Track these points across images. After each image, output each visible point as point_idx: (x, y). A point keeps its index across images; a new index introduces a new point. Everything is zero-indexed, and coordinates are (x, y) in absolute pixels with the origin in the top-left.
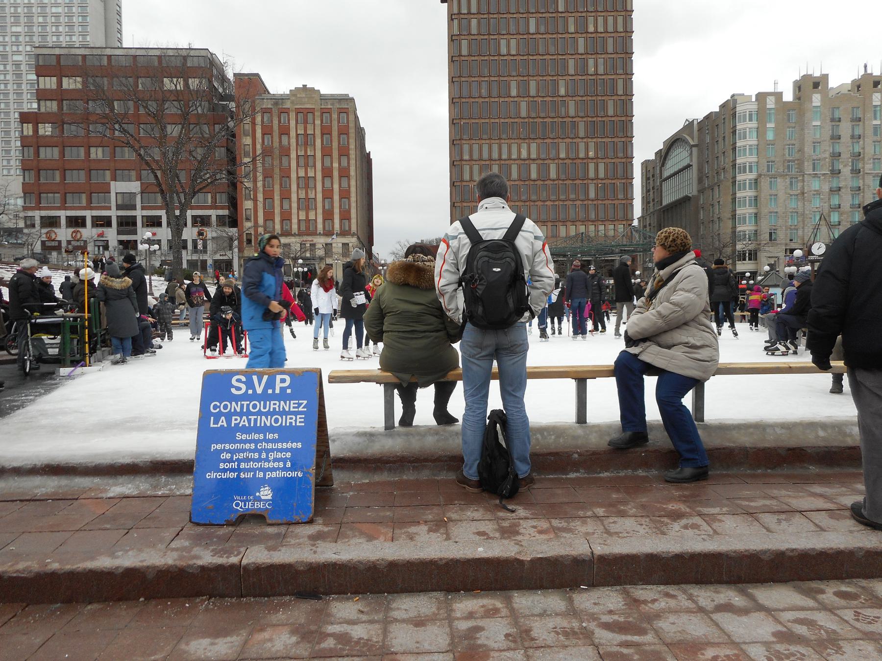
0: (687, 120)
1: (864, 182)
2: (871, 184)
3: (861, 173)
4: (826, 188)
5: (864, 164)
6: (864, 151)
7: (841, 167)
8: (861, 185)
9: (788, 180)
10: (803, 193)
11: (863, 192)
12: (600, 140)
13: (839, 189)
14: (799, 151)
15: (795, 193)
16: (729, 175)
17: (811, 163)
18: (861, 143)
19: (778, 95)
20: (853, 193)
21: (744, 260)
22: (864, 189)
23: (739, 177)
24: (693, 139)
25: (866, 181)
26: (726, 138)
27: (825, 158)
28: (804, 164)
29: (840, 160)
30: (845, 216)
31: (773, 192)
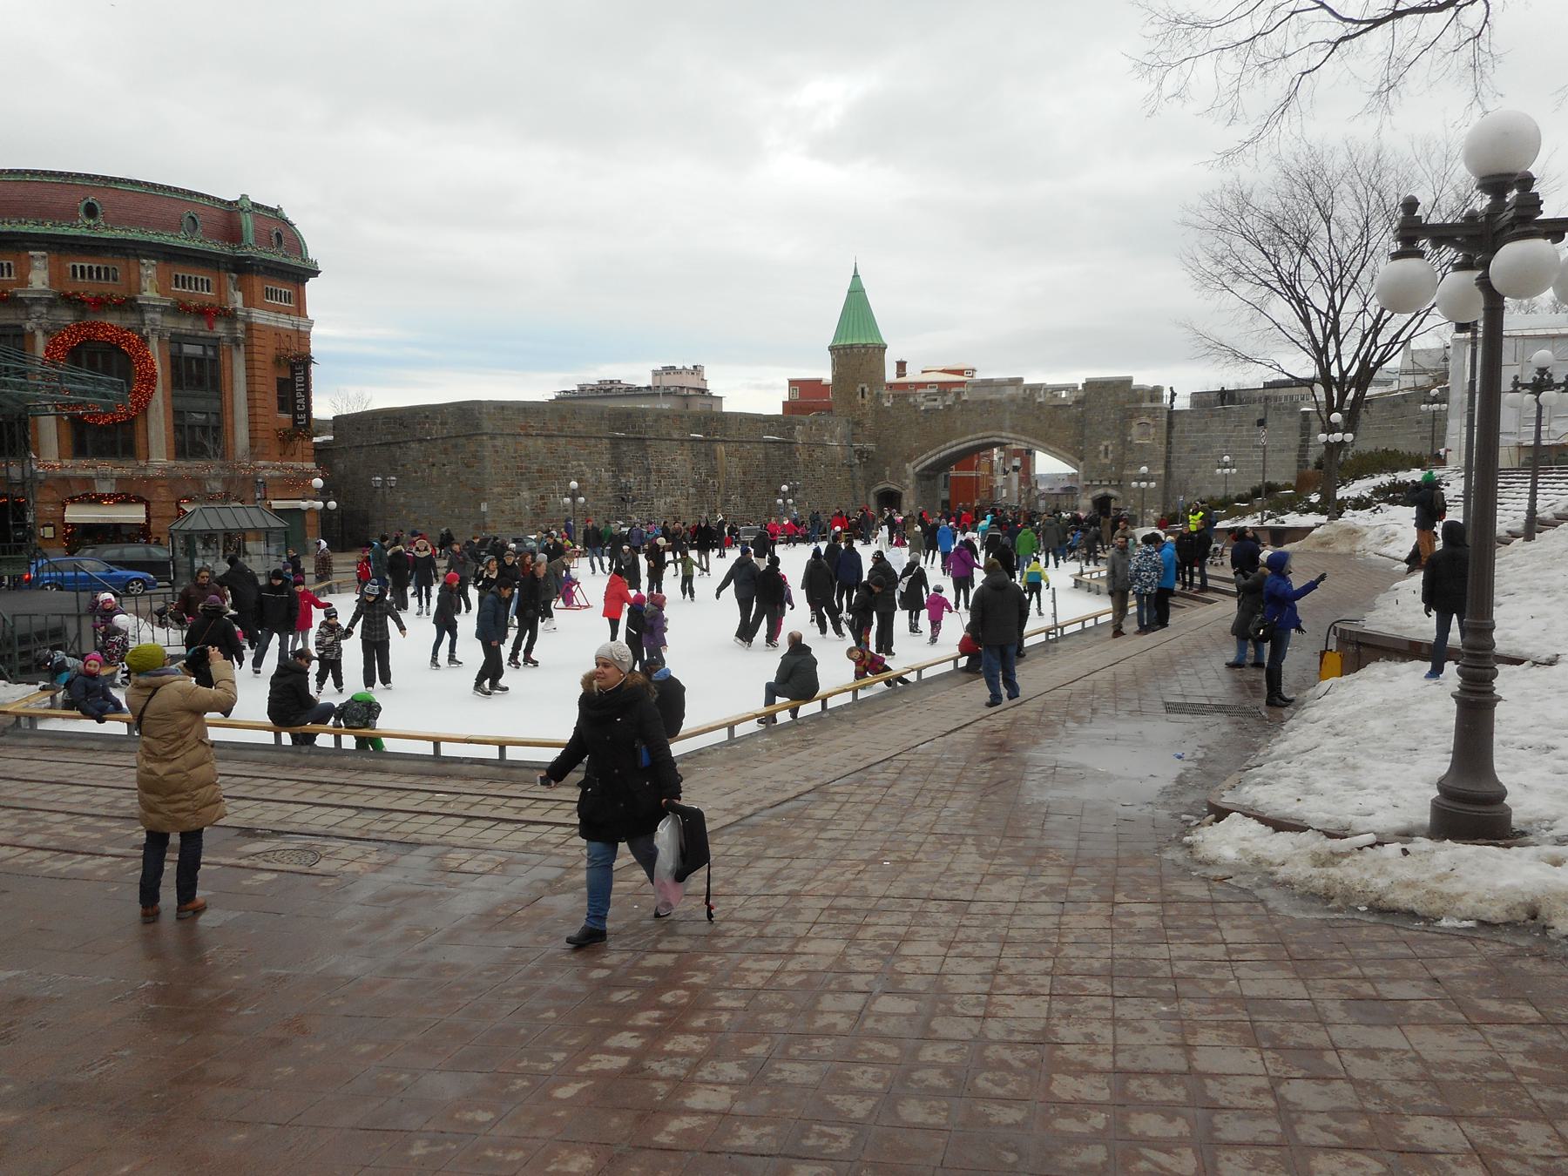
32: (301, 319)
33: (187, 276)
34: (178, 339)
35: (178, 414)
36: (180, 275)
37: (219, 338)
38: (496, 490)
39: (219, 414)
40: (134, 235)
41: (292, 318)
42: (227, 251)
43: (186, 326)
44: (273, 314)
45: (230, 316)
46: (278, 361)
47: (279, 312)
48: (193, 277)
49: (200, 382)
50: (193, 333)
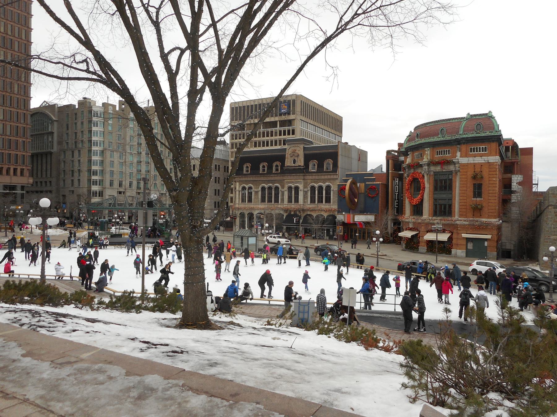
0: (45, 101)
4: (135, 160)
7: (142, 151)
9: (119, 154)
10: (125, 162)
12: (7, 108)
13: (141, 162)
14: (123, 139)
15: (121, 161)
16: (86, 145)
17: (129, 147)
19: (114, 106)
21: (96, 196)
23: (94, 148)
24: (54, 116)
26: (85, 123)
27: (135, 145)
31: (112, 159)
32: (489, 157)
33: (441, 150)
34: (436, 174)
35: (435, 200)
36: (438, 151)
37: (452, 171)
38: (552, 237)
39: (451, 199)
40: (423, 141)
41: (483, 158)
42: (454, 138)
43: (438, 168)
44: (471, 158)
45: (454, 163)
46: (474, 177)
47: (475, 157)
48: (443, 150)
49: (445, 188)
50: (441, 171)
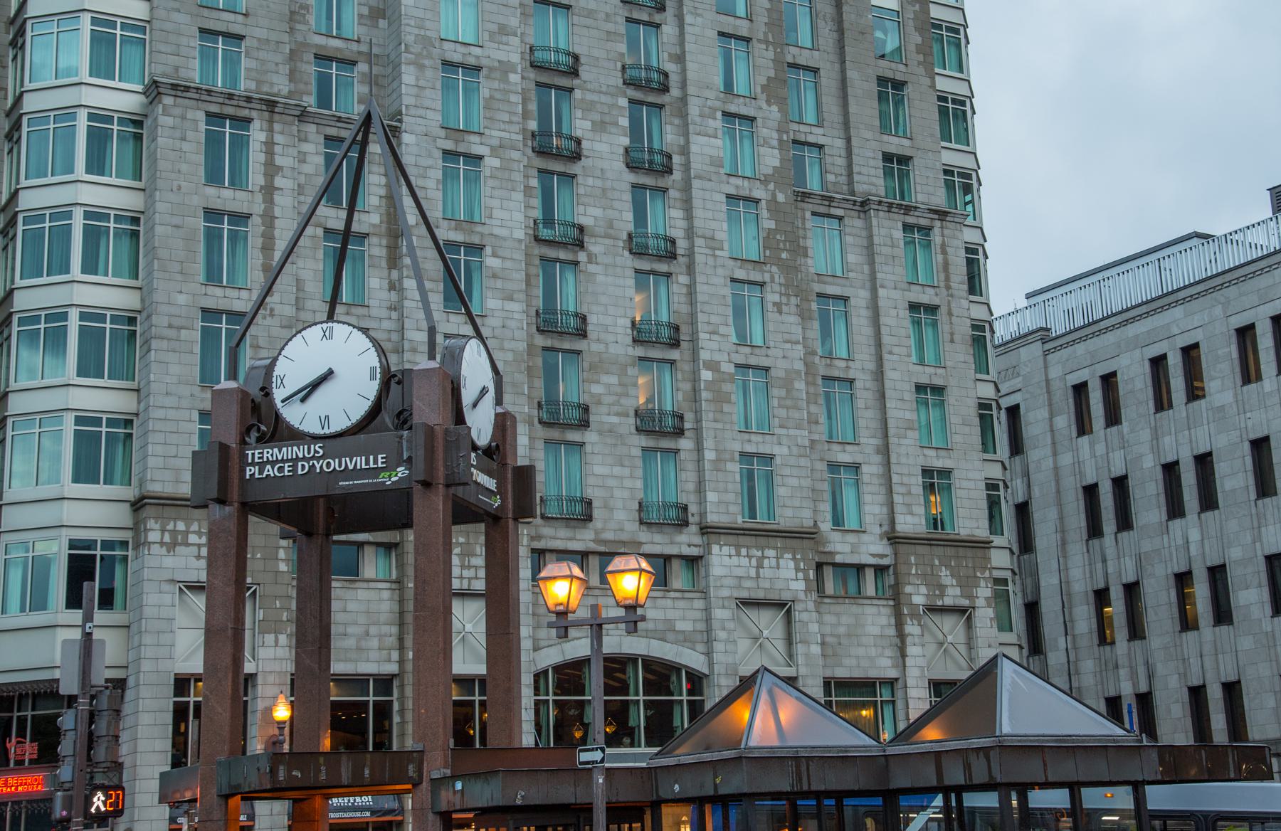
1: (689, 217)
2: (721, 230)
3: (677, 175)
5: (686, 135)
6: (684, 71)
7: (581, 126)
8: (677, 233)
11: (690, 269)
18: (669, 30)
20: (645, 265)
22: (691, 254)
25: (698, 213)
27: (505, 68)
28: (397, 76)
29: (578, 94)
30: (613, 380)
